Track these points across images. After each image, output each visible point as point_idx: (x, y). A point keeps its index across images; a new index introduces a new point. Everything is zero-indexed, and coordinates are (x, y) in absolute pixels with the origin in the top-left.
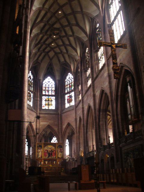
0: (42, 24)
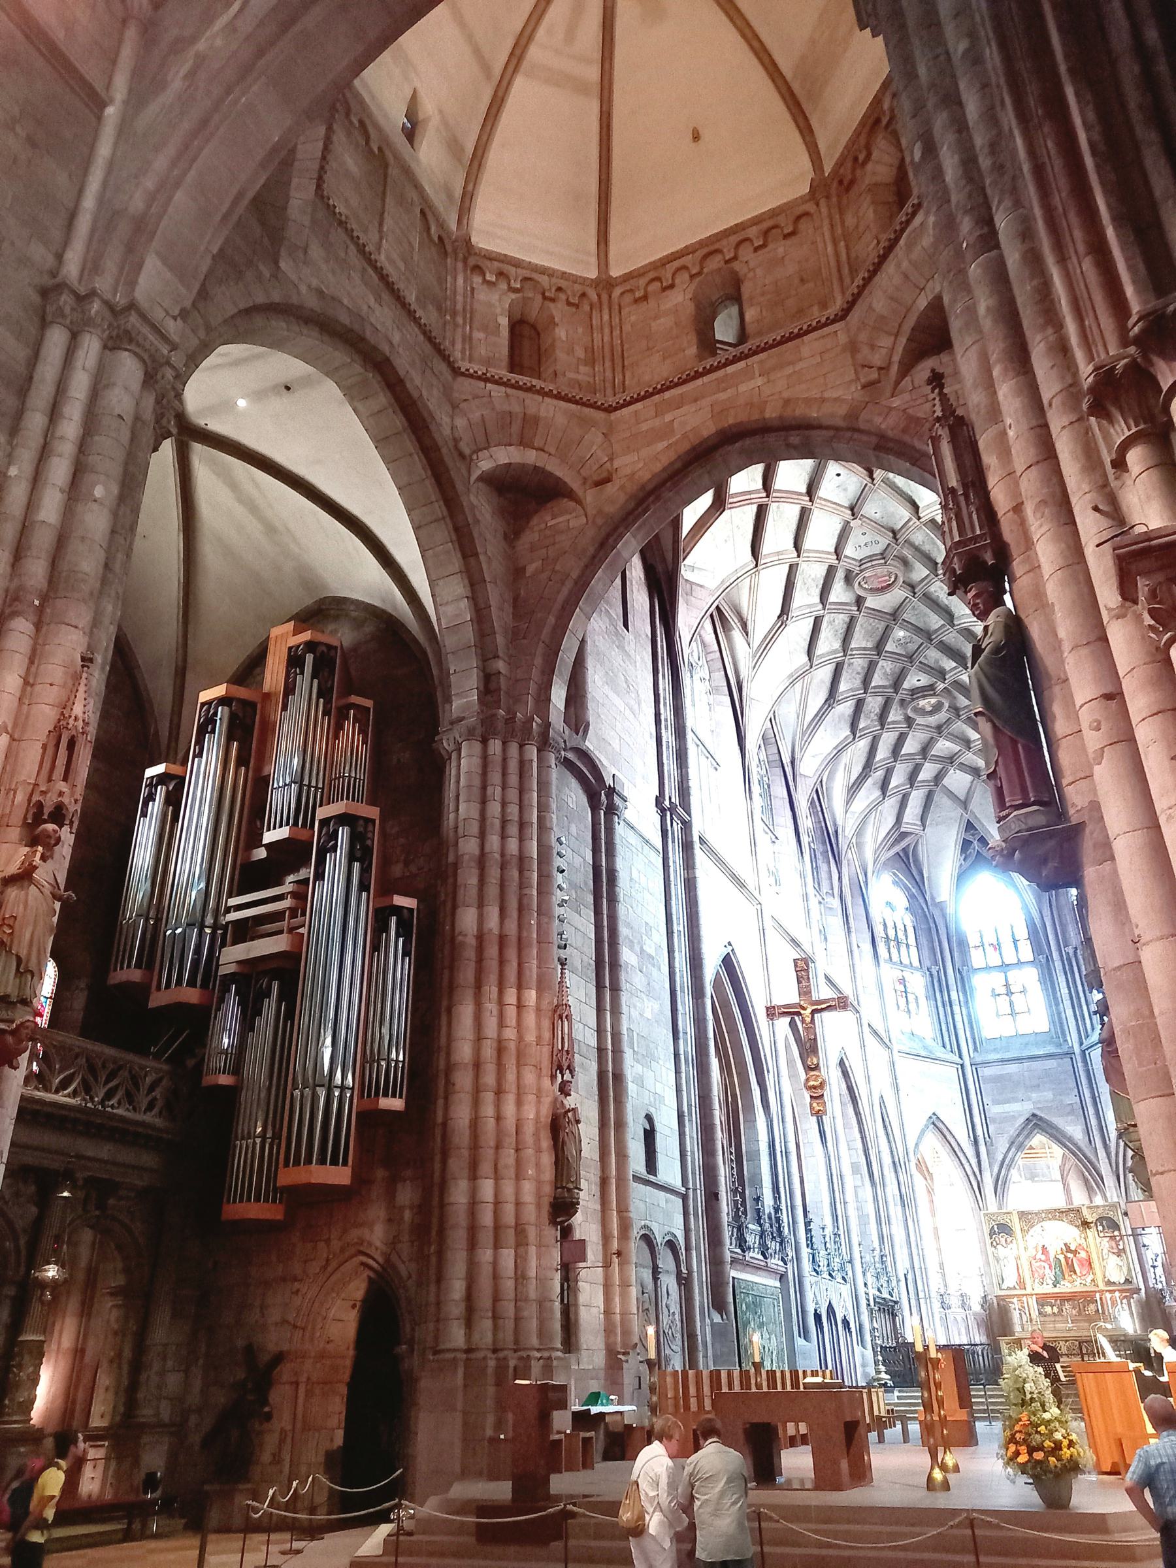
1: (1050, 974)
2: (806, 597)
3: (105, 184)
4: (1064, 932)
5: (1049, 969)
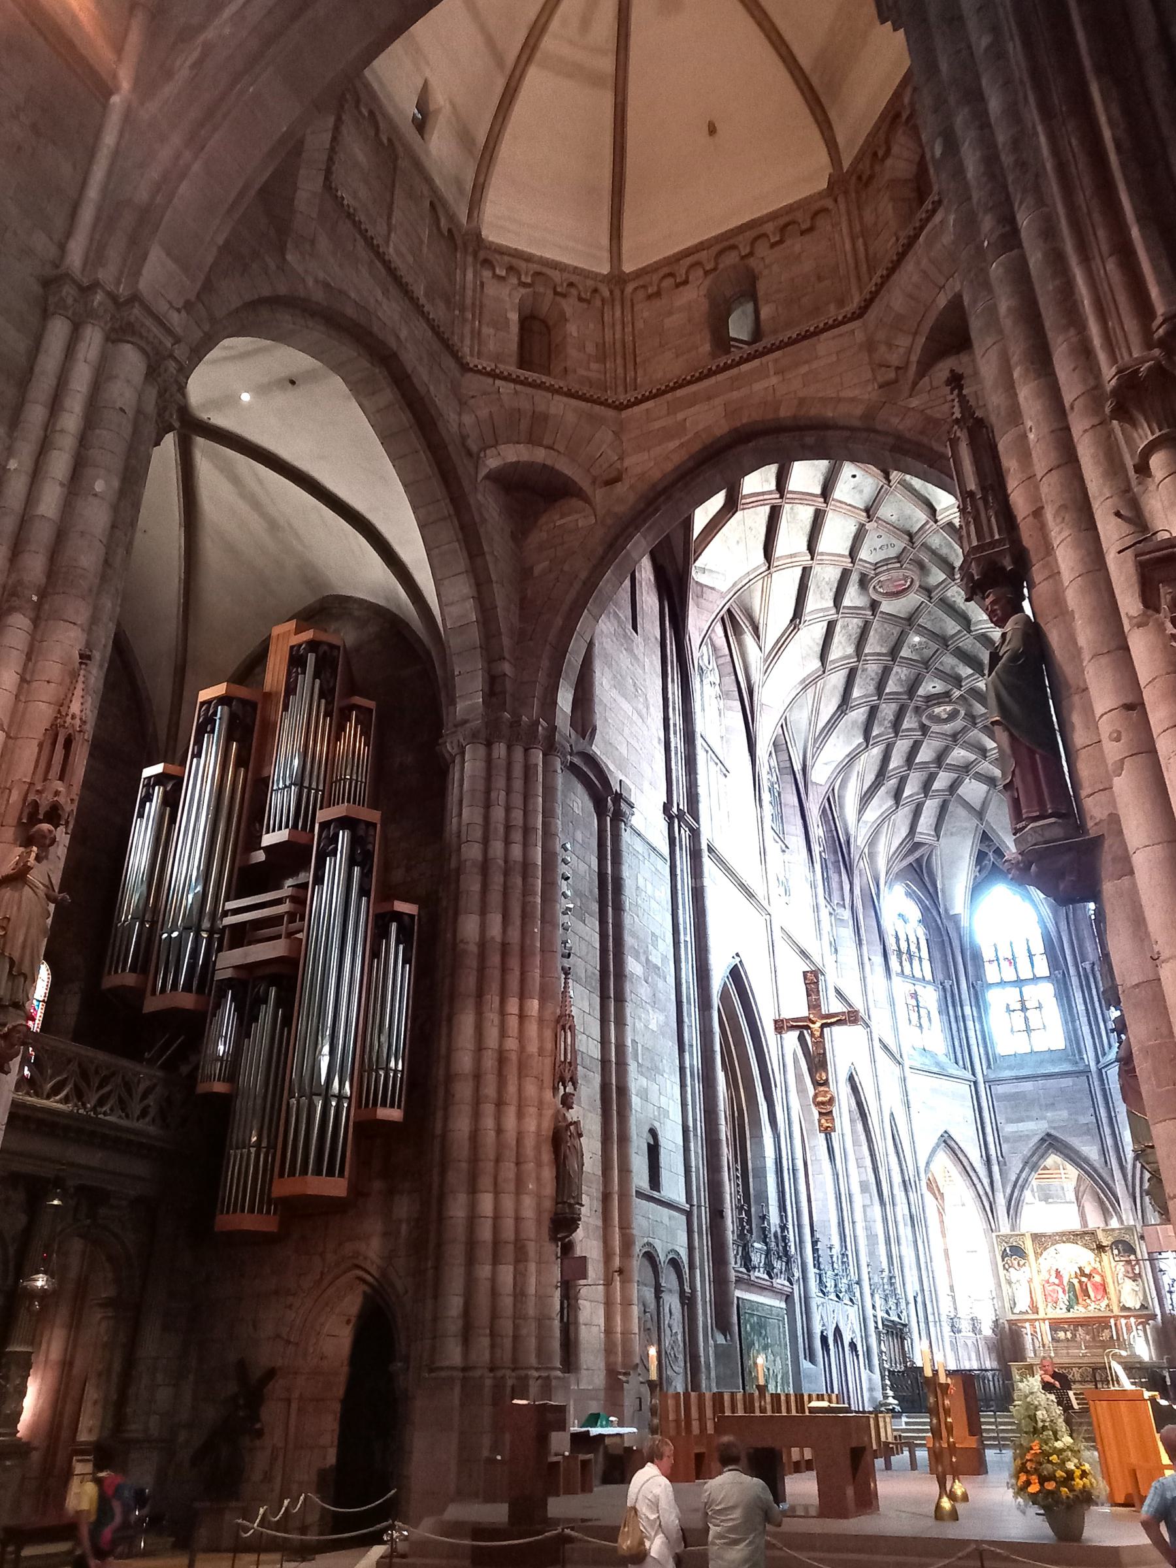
0: (858, 715)
1: (1067, 990)
2: (819, 601)
3: (110, 173)
4: (1081, 947)
5: (1065, 984)
